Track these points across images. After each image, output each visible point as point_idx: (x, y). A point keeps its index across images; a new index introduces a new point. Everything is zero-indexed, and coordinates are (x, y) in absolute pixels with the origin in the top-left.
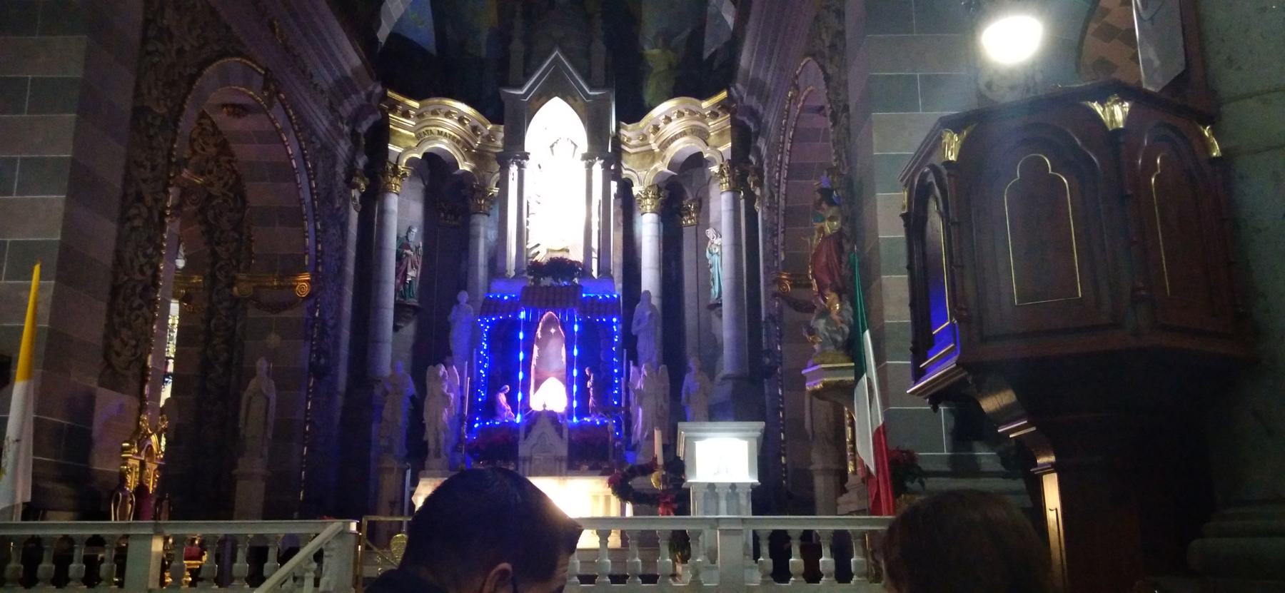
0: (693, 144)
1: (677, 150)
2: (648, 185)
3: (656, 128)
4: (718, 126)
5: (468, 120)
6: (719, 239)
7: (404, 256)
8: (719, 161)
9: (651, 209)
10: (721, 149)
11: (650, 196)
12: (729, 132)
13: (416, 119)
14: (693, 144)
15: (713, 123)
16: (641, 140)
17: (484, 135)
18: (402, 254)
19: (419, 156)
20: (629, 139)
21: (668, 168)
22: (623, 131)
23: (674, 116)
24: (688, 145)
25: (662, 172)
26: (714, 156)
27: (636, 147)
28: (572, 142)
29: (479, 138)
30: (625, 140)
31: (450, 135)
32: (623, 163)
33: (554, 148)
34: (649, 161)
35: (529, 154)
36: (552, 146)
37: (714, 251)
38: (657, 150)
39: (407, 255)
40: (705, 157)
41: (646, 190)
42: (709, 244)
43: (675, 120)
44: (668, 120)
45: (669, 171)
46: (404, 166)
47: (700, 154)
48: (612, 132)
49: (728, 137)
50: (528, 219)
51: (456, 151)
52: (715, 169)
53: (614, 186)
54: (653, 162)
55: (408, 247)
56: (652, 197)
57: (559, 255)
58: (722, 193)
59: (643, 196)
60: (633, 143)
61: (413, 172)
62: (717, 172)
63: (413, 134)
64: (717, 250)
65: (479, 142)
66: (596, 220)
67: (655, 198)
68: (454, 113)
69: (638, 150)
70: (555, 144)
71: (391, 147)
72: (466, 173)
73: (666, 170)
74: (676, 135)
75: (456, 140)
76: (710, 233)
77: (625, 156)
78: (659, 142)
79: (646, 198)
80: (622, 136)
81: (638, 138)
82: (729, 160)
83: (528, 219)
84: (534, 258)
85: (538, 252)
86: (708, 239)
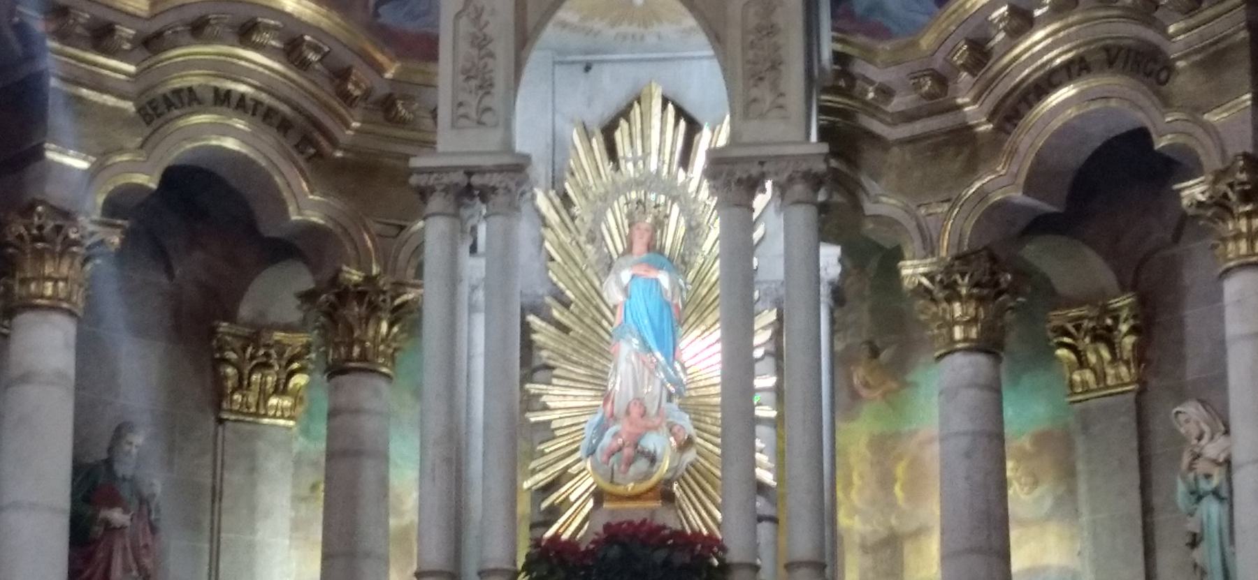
0: (1113, 103)
1: (1057, 124)
2: (954, 252)
3: (980, 53)
4: (1202, 37)
5: (316, 49)
6: (1221, 441)
7: (98, 530)
8: (1212, 161)
9: (965, 340)
10: (1213, 117)
11: (964, 291)
12: (1245, 53)
13: (141, 53)
14: (1113, 103)
15: (1182, 25)
16: (930, 96)
17: (372, 99)
18: (93, 519)
19: (148, 180)
20: (886, 92)
21: (1029, 189)
22: (859, 67)
23: (1040, 6)
24: (1094, 106)
25: (1003, 205)
26: (1192, 143)
27: (908, 117)
28: (680, 113)
29: (357, 112)
30: (871, 95)
31: (258, 103)
32: (865, 180)
33: (618, 135)
34: (956, 166)
35: (527, 158)
36: (609, 132)
37: (1204, 486)
38: (986, 127)
39: (109, 528)
40: (1160, 143)
41: (948, 270)
42: (1186, 459)
43: (1046, 20)
44: (1022, 21)
45: (1030, 201)
46: (96, 216)
47: (1140, 137)
48: (822, 70)
49: (1241, 73)
50: (533, 388)
51: (276, 158)
52: (1194, 191)
53: (830, 257)
54: (971, 170)
55: (114, 500)
56: (970, 296)
57: (636, 511)
58: (1228, 271)
59: (940, 295)
60: (898, 103)
61: (130, 238)
62: (1202, 198)
63: (129, 106)
64: (1215, 482)
65: (355, 125)
66: (765, 381)
67: (981, 300)
68: (268, 28)
69: (918, 127)
70: (623, 123)
71: (52, 155)
72: (311, 230)
73: (1018, 196)
74: (1054, 71)
75: (276, 121)
76: (1191, 415)
77: (870, 156)
78: (990, 101)
79: (949, 300)
80: (859, 82)
81: (917, 87)
82: (1246, 156)
83: (533, 388)
84: (548, 525)
85: (566, 503)
86: (1182, 441)
